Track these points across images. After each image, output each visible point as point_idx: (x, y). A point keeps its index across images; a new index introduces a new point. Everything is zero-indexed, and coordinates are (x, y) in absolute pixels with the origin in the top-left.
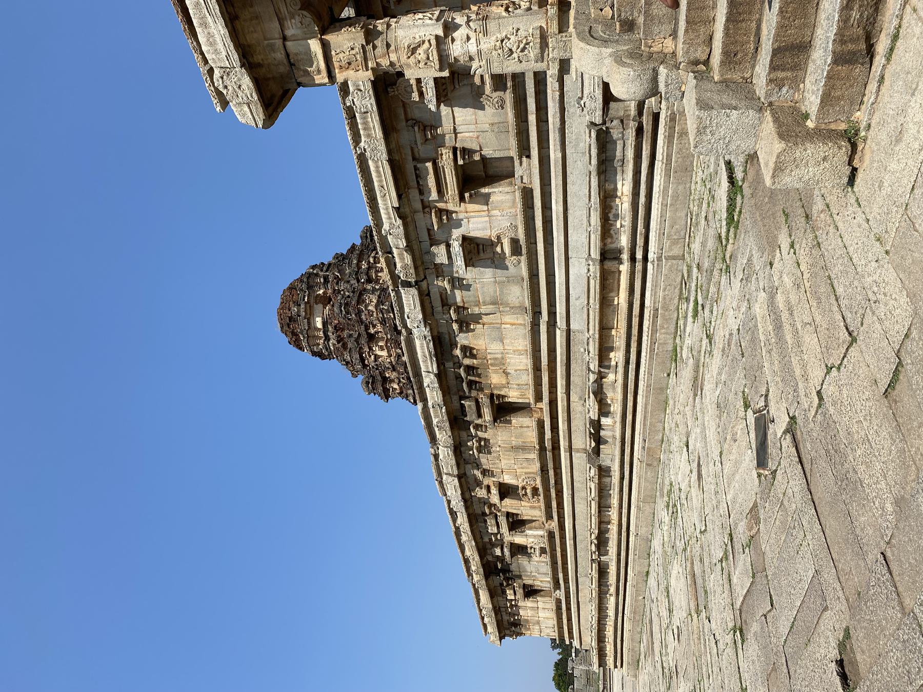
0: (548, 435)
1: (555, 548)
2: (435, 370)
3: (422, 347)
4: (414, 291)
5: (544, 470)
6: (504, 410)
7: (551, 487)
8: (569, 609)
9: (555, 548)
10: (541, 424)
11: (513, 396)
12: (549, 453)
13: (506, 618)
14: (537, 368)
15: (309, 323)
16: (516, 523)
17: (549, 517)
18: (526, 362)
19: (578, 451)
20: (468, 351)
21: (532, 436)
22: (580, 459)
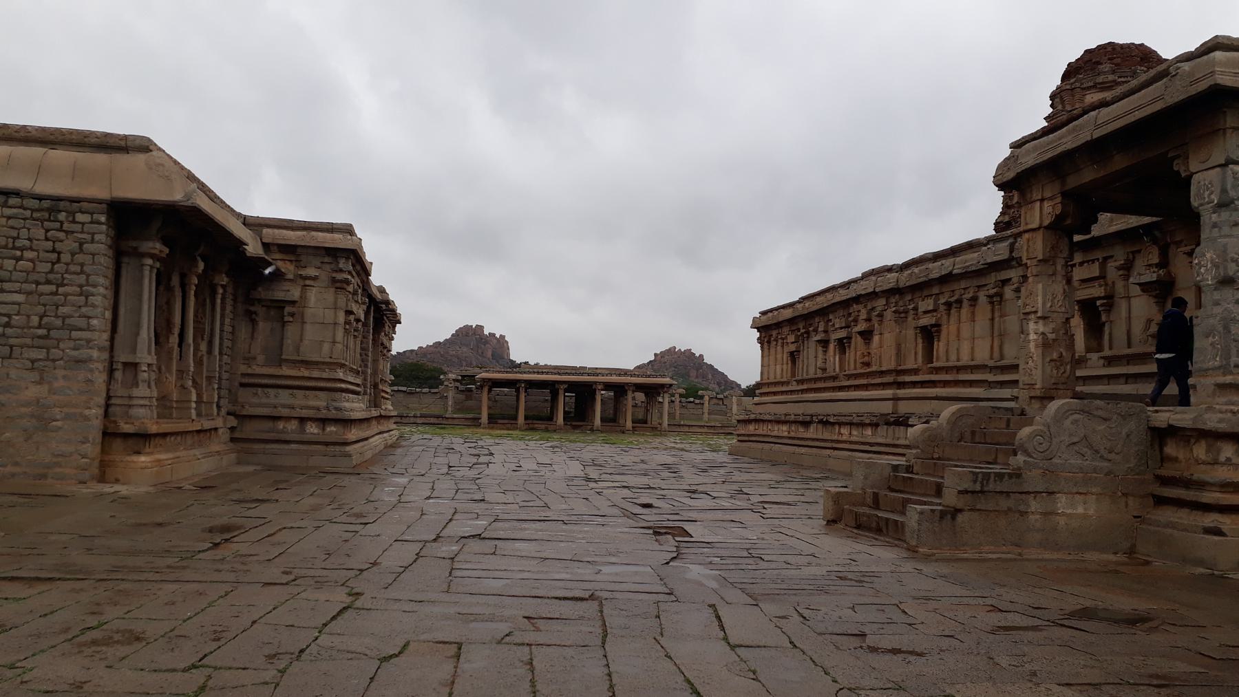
0: (908, 379)
1: (826, 382)
2: (955, 272)
3: (972, 259)
4: (1006, 256)
5: (882, 373)
6: (929, 335)
7: (869, 378)
8: (782, 393)
9: (826, 382)
10: (915, 371)
11: (940, 347)
12: (897, 379)
13: (774, 333)
14: (959, 369)
15: (1089, 88)
16: (842, 345)
17: (849, 377)
18: (965, 360)
19: (895, 406)
20: (974, 300)
21: (910, 365)
22: (887, 407)
